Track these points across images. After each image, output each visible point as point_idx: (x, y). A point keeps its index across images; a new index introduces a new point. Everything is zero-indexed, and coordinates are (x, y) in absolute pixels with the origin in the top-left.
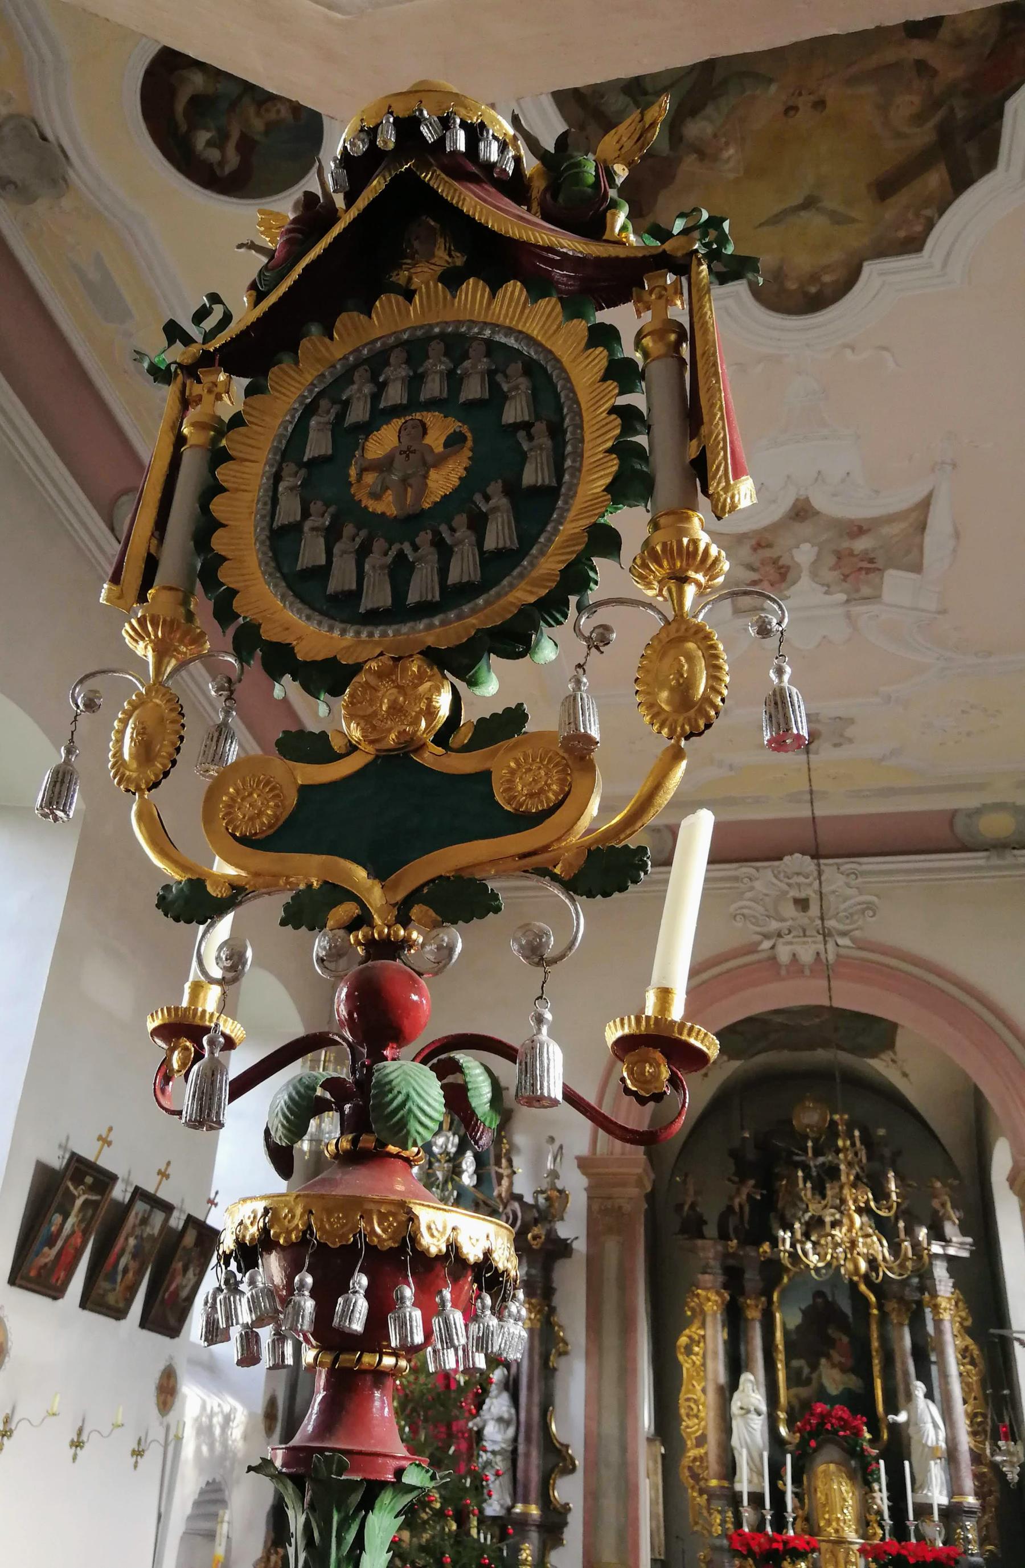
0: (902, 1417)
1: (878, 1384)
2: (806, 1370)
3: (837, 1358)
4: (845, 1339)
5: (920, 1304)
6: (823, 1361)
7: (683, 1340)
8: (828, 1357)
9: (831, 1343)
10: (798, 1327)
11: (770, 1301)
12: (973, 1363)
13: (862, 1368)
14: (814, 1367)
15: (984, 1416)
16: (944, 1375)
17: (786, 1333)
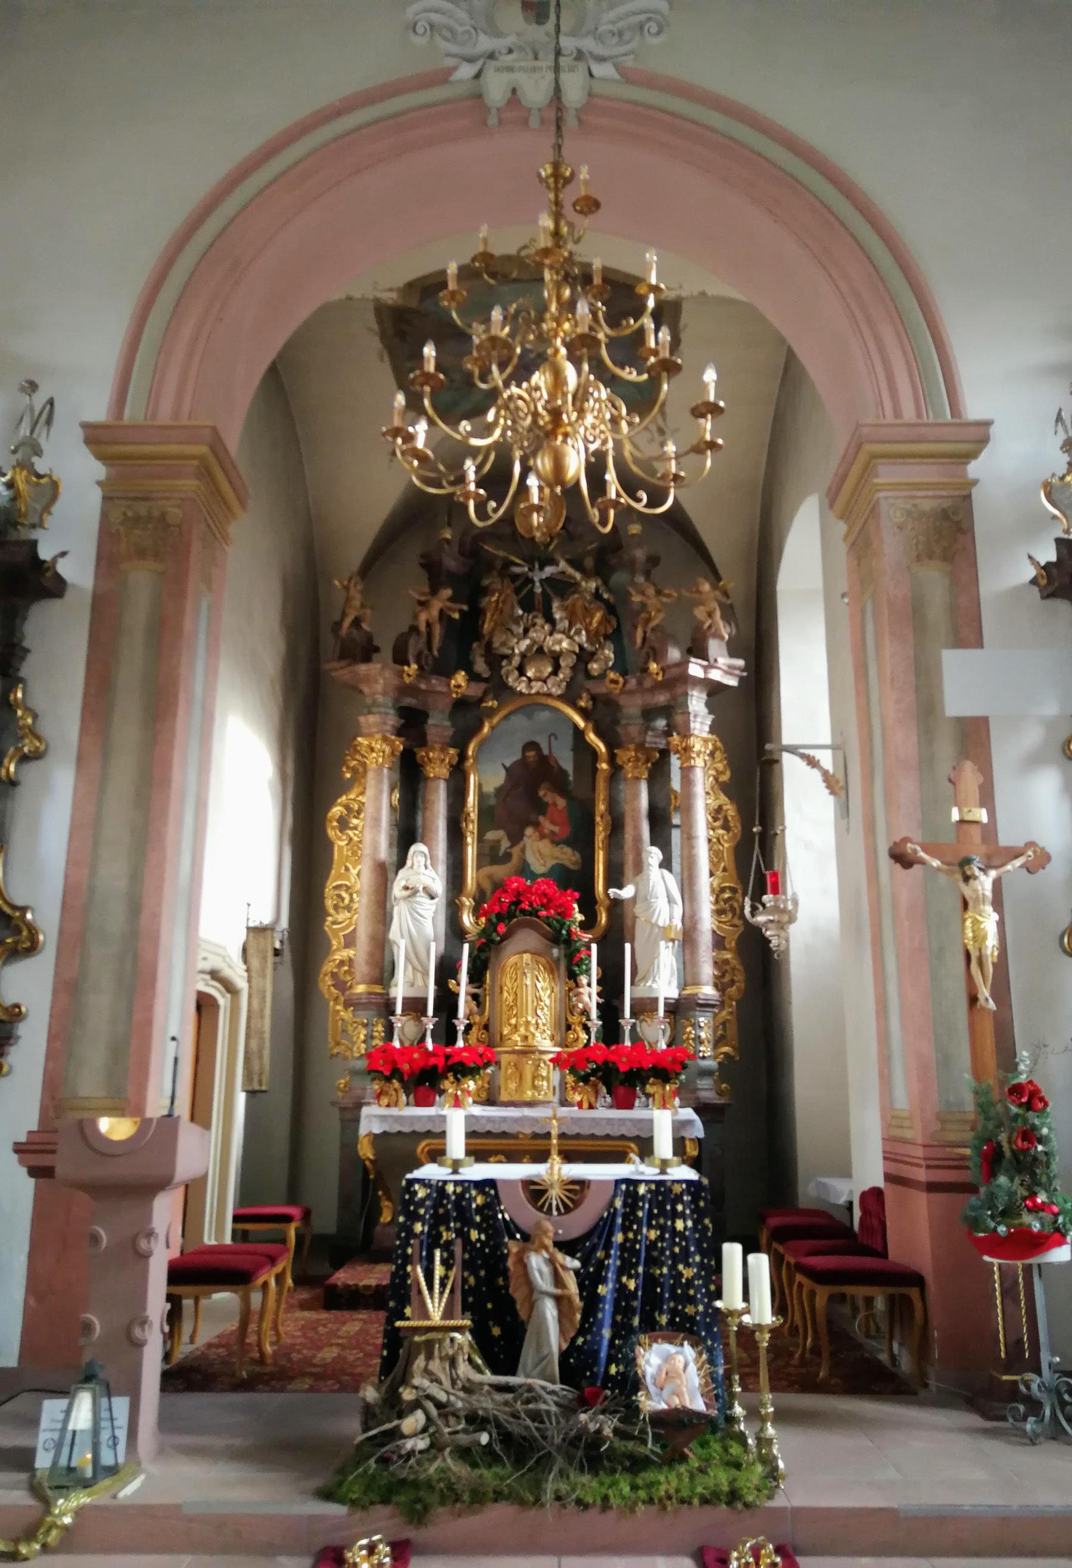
0: (627, 892)
1: (600, 857)
2: (505, 844)
3: (548, 826)
4: (561, 803)
5: (665, 753)
6: (529, 831)
7: (337, 810)
8: (537, 825)
9: (541, 807)
10: (499, 790)
11: (462, 757)
12: (726, 827)
13: (581, 838)
14: (516, 838)
15: (733, 890)
16: (689, 838)
17: (482, 796)
